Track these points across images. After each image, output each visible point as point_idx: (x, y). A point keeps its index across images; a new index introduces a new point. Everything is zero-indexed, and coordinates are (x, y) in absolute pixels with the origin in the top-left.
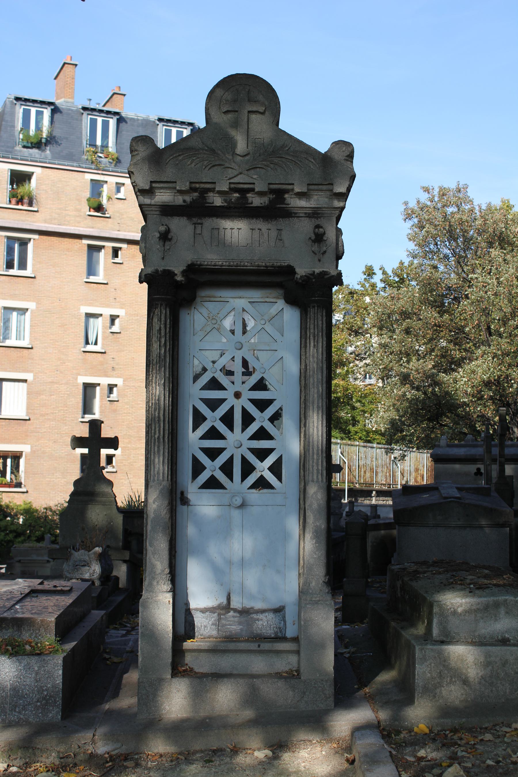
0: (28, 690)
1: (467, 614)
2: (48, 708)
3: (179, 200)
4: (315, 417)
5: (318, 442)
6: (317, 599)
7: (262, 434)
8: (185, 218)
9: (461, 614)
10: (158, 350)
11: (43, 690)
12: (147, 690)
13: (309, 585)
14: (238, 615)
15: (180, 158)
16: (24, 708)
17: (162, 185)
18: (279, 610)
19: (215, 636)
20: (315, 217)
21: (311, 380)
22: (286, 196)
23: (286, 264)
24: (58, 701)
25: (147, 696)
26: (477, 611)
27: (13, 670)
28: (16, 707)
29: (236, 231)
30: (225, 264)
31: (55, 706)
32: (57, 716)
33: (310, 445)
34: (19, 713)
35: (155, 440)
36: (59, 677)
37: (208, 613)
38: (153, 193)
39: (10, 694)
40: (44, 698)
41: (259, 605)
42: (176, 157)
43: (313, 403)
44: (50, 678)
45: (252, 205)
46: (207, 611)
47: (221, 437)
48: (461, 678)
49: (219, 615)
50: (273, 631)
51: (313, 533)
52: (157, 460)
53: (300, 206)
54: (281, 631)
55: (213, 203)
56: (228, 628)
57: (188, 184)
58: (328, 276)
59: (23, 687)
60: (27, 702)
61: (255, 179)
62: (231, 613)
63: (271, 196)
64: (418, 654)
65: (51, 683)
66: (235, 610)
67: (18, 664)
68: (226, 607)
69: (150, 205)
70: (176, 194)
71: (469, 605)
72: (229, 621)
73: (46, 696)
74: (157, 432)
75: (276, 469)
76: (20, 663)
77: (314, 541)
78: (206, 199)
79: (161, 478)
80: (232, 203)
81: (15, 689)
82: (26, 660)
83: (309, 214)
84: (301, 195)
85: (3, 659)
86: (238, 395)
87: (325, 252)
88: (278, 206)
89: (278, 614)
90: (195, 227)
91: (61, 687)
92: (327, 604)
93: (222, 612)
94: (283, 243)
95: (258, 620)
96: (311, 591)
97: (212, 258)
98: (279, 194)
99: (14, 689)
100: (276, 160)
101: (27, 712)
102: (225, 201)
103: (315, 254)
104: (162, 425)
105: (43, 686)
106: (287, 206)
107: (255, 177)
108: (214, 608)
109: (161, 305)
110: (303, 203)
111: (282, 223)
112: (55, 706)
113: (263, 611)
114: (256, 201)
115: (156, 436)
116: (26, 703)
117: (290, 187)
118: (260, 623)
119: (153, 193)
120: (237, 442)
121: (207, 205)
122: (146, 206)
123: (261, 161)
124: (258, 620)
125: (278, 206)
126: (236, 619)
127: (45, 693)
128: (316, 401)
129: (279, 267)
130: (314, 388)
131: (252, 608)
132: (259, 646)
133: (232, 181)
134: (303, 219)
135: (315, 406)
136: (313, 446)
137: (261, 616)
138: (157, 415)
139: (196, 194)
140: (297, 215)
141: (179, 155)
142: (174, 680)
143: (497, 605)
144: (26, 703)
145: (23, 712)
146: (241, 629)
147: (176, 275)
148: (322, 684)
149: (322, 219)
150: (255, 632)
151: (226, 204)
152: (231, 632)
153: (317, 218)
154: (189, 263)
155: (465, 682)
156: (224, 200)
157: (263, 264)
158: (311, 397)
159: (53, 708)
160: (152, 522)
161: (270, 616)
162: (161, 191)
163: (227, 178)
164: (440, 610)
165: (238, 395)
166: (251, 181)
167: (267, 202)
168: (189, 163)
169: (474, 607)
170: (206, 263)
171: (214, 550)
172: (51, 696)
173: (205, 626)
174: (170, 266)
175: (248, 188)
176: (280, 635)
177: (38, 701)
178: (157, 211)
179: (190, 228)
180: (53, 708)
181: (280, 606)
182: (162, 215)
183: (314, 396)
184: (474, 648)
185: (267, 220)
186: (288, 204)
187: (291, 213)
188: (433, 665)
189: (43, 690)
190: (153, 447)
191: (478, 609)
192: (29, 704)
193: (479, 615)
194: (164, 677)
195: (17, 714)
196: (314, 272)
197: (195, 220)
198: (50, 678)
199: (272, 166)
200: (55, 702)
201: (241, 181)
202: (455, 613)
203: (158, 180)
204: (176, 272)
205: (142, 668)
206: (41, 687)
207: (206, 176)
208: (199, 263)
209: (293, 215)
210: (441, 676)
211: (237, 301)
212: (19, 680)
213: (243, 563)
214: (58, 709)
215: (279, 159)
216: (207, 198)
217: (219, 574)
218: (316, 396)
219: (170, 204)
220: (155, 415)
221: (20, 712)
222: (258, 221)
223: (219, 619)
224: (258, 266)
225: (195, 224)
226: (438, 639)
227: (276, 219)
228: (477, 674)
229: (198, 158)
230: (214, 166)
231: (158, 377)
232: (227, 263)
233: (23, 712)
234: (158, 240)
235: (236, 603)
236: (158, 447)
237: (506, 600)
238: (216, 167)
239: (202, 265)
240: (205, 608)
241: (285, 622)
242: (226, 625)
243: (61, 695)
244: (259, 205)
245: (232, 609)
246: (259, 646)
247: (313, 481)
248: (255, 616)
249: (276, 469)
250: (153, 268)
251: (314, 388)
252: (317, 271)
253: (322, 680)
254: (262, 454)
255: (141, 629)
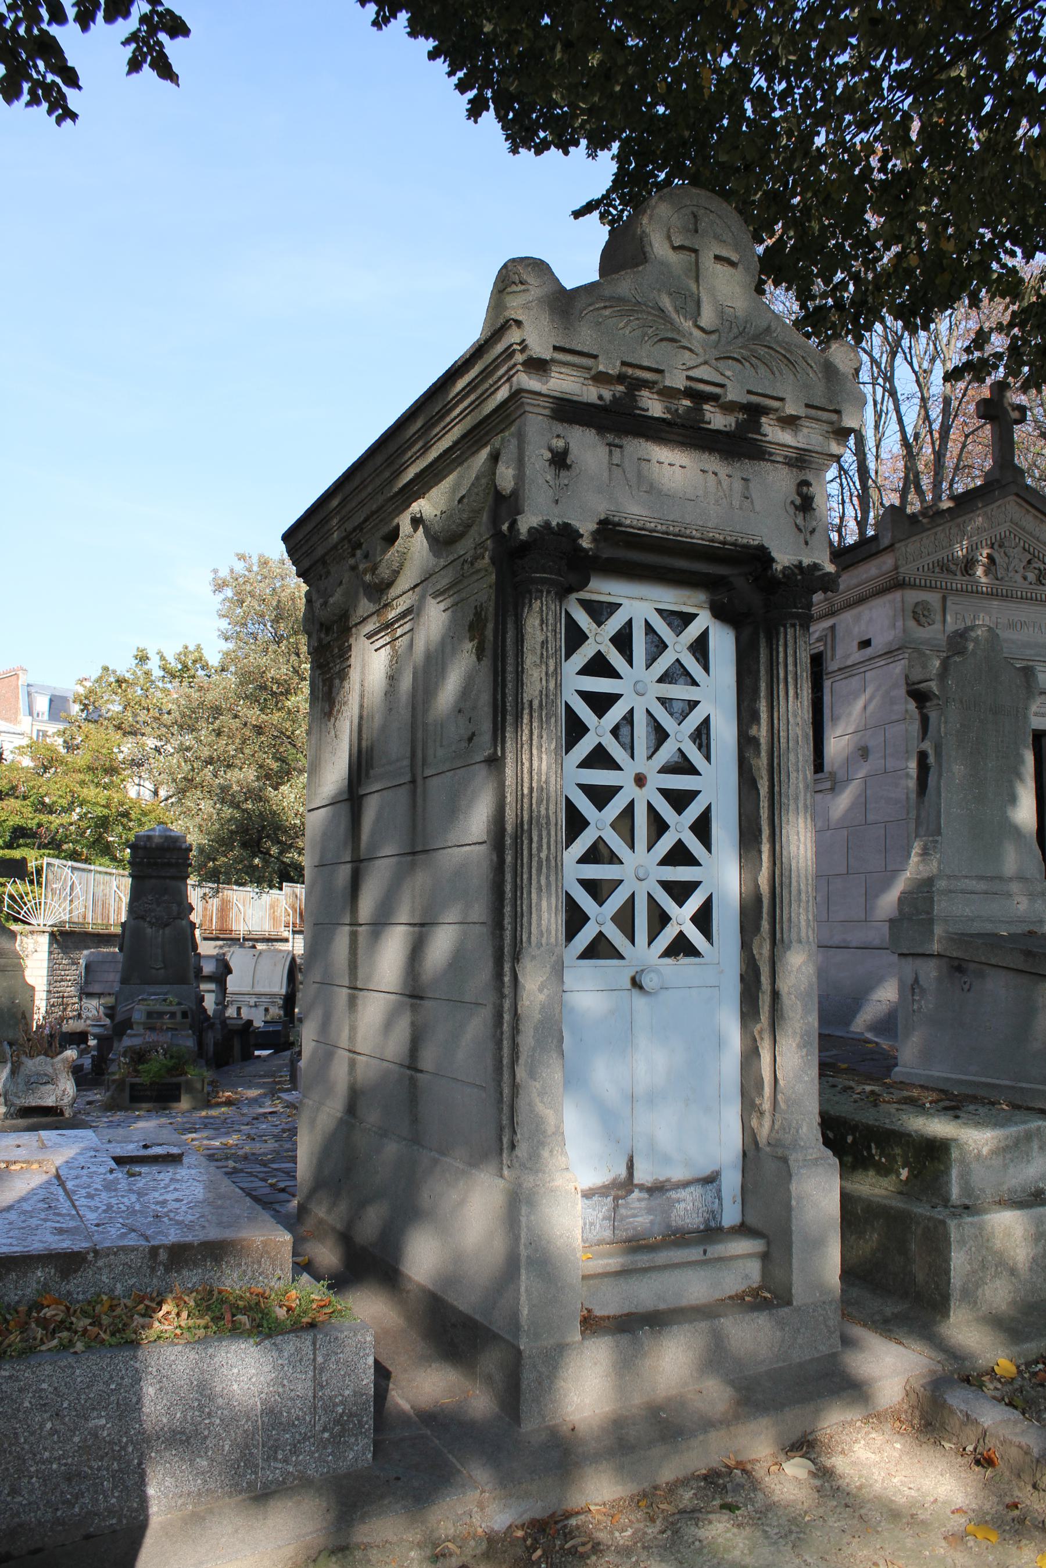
0: (301, 1409)
1: (994, 1157)
2: (345, 1442)
3: (591, 394)
4: (801, 825)
5: (806, 870)
6: (814, 1156)
7: (679, 855)
8: (593, 431)
9: (986, 1158)
10: (544, 682)
11: (335, 1405)
12: (538, 1371)
13: (797, 1132)
14: (646, 1196)
15: (607, 312)
16: (295, 1451)
17: (569, 358)
18: (711, 1180)
19: (608, 1240)
20: (798, 467)
21: (792, 757)
22: (763, 420)
23: (756, 543)
24: (367, 1422)
25: (540, 1383)
26: (1006, 1149)
27: (266, 1369)
28: (275, 1449)
29: (673, 467)
30: (659, 527)
31: (361, 1433)
32: (364, 1454)
33: (793, 876)
34: (285, 1461)
35: (540, 862)
36: (368, 1371)
37: (595, 1198)
38: (545, 371)
39: (263, 1422)
40: (337, 1422)
41: (677, 1174)
42: (598, 309)
43: (797, 799)
44: (349, 1375)
45: (709, 426)
46: (594, 1195)
47: (614, 859)
48: (1006, 1267)
49: (616, 1199)
50: (701, 1219)
51: (802, 1037)
52: (544, 904)
53: (782, 441)
54: (714, 1218)
55: (647, 410)
56: (631, 1223)
57: (618, 363)
58: (820, 573)
59: (289, 1403)
60: (300, 1434)
61: (728, 378)
62: (636, 1194)
63: (741, 416)
64: (954, 1235)
65: (351, 1388)
66: (642, 1187)
67: (275, 1354)
68: (626, 1185)
69: (539, 394)
70: (586, 382)
71: (995, 1141)
72: (631, 1209)
73: (341, 1416)
74: (545, 847)
75: (703, 919)
76: (281, 1351)
77: (805, 1050)
78: (636, 401)
79: (553, 940)
80: (679, 416)
81: (272, 1411)
82: (291, 1344)
83: (791, 458)
84: (790, 422)
85: (243, 1346)
86: (640, 780)
87: (813, 532)
88: (750, 435)
89: (710, 1187)
90: (611, 451)
91: (372, 1392)
92: (829, 1164)
93: (620, 1193)
94: (752, 503)
95: (678, 1201)
96: (802, 1144)
97: (635, 512)
98: (753, 413)
99: (270, 1411)
100: (762, 351)
101: (301, 1457)
102: (668, 410)
103: (800, 530)
104: (553, 833)
105: (336, 1396)
106: (764, 438)
107: (728, 373)
108: (605, 1187)
109: (549, 592)
110: (786, 437)
111: (749, 468)
112: (361, 1433)
113: (686, 1184)
114: (718, 420)
115: (543, 855)
116: (297, 1437)
117: (776, 404)
118: (682, 1205)
119: (545, 371)
120: (640, 869)
121: (638, 412)
122: (530, 396)
123: (740, 348)
124: (678, 1201)
125: (750, 435)
126: (643, 1204)
127: (340, 1410)
128: (802, 794)
129: (744, 546)
130: (798, 771)
131: (668, 1180)
132: (705, 1252)
133: (691, 373)
134: (779, 466)
135: (801, 805)
136: (799, 876)
137: (682, 1194)
138: (543, 812)
139: (621, 388)
140: (772, 458)
141: (605, 307)
142: (586, 1343)
143: (1028, 1137)
144: (297, 1437)
145: (294, 1459)
146: (652, 1222)
147: (582, 536)
148: (825, 1309)
149: (807, 471)
150: (674, 1224)
151: (668, 416)
152: (635, 1229)
153: (801, 468)
154: (602, 517)
155: (1013, 1272)
156: (666, 408)
157: (721, 538)
158: (792, 788)
159: (357, 1440)
160: (536, 1029)
161: (696, 1191)
162: (563, 370)
163: (684, 367)
164: (961, 1154)
165: (640, 780)
166: (718, 379)
167: (733, 425)
168: (621, 325)
169: (1002, 1144)
170: (628, 522)
171: (605, 1075)
172: (351, 1415)
173: (591, 1224)
174: (569, 518)
175: (711, 393)
176: (713, 1224)
177: (325, 1430)
178: (545, 408)
179: (602, 451)
180: (357, 1440)
181: (712, 1172)
182: (552, 418)
183: (797, 787)
184: (1018, 1213)
185: (726, 459)
186: (765, 435)
187: (764, 452)
188: (973, 1249)
189: (335, 1405)
190: (534, 877)
191: (1007, 1146)
192: (305, 1438)
193: (1008, 1156)
194: (569, 1340)
195: (280, 1465)
196: (800, 562)
197: (610, 437)
198: (349, 1375)
199: (754, 360)
200: (361, 1425)
201: (706, 378)
202: (979, 1155)
203: (567, 346)
204: (581, 531)
205: (529, 1329)
206: (330, 1398)
207: (647, 355)
208: (616, 519)
209: (767, 457)
210: (984, 1266)
211: (637, 604)
212: (281, 1390)
213: (652, 1099)
214: (366, 1440)
215: (766, 350)
216: (638, 398)
217: (609, 1121)
218: (801, 786)
219: (575, 398)
220: (539, 812)
221: (286, 1461)
222: (713, 459)
223: (616, 1208)
224: (712, 541)
225: (609, 445)
226: (959, 1203)
227: (739, 459)
228: (1028, 1254)
229: (638, 319)
230: (661, 340)
231: (545, 736)
232: (664, 528)
233: (294, 1459)
234: (547, 463)
235: (643, 1175)
236: (548, 878)
237: (1040, 1127)
238: (664, 343)
239: (620, 524)
240: (591, 1189)
241: (720, 1199)
242: (627, 1217)
243: (372, 1409)
244: (722, 428)
245: (637, 1186)
246: (705, 1252)
247: (800, 941)
248: (673, 1195)
249: (703, 919)
250: (540, 518)
251: (798, 771)
252: (806, 561)
253: (824, 1303)
254: (681, 891)
255: (526, 1248)
